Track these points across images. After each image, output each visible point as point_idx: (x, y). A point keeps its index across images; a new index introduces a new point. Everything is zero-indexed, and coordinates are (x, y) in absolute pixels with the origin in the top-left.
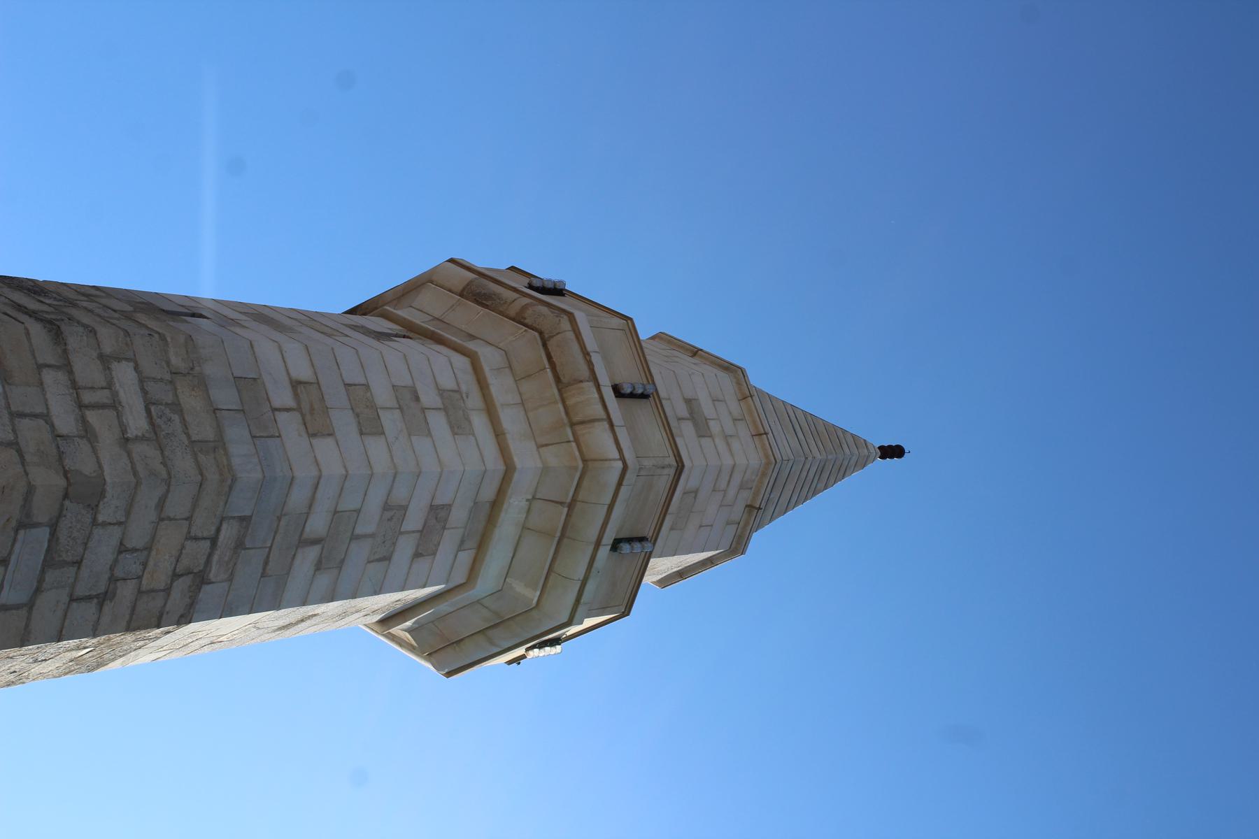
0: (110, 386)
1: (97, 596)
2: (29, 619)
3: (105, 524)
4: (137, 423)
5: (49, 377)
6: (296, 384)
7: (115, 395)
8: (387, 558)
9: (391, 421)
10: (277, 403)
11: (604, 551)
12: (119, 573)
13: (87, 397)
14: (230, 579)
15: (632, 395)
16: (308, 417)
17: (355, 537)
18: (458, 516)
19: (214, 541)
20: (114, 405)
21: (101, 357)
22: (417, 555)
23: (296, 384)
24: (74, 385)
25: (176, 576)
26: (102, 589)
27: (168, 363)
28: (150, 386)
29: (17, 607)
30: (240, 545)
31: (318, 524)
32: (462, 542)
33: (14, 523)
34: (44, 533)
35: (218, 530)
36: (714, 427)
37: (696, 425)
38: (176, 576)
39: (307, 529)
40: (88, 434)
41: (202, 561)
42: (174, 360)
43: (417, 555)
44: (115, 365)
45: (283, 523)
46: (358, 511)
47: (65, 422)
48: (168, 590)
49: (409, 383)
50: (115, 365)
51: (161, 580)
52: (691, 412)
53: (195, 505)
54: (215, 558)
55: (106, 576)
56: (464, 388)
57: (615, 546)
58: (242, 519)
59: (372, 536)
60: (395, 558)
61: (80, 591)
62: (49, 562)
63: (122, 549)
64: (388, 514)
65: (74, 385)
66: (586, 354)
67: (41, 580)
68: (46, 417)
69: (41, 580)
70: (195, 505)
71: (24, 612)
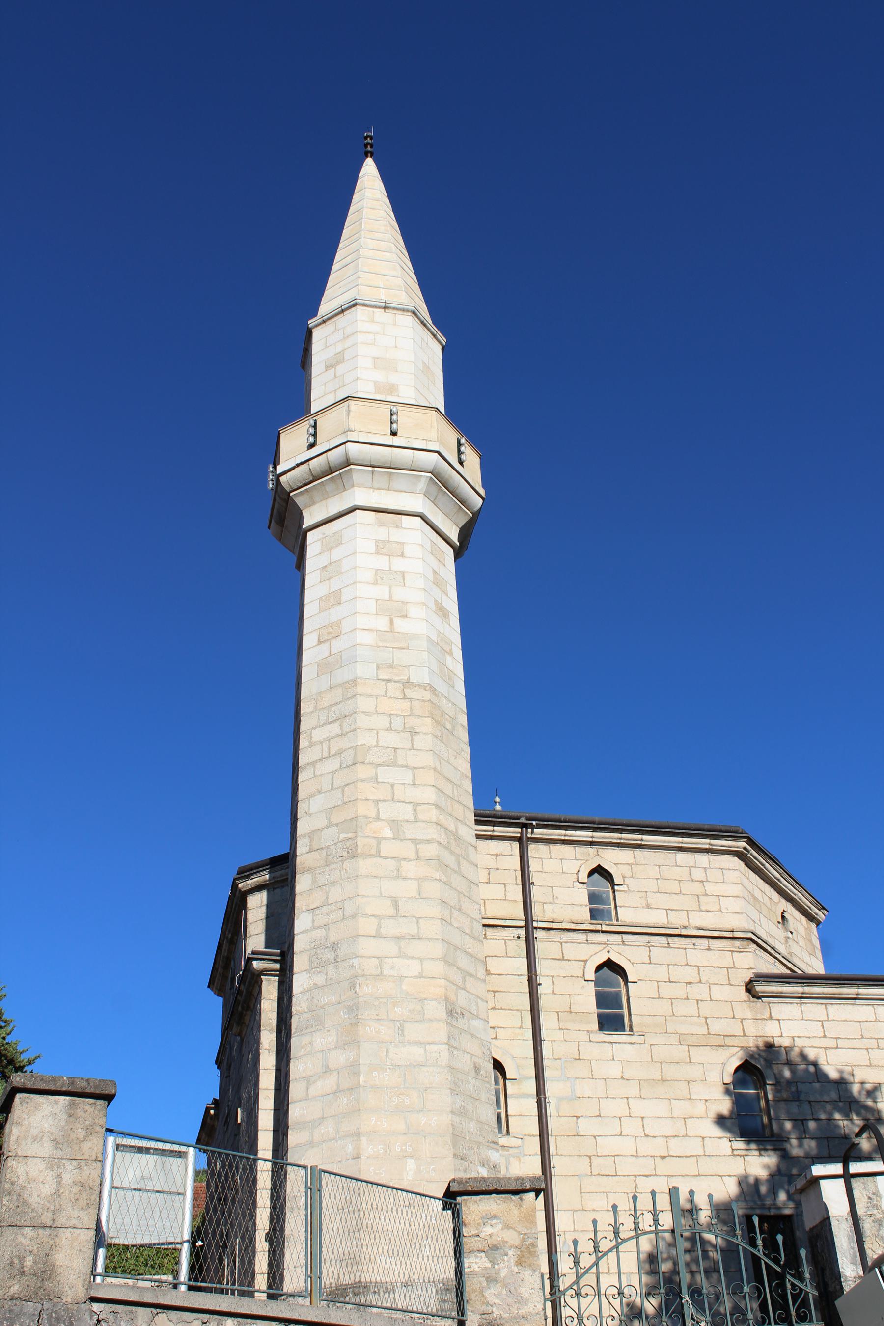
0: (321, 742)
1: (411, 736)
2: (420, 768)
3: (377, 741)
4: (335, 729)
5: (318, 773)
6: (320, 642)
7: (325, 740)
8: (403, 573)
9: (335, 584)
10: (327, 653)
11: (396, 441)
12: (401, 728)
13: (326, 754)
14: (407, 667)
15: (315, 435)
16: (334, 635)
17: (391, 599)
18: (382, 533)
19: (388, 681)
20: (328, 739)
21: (310, 746)
22: (402, 555)
23: (320, 642)
24: (321, 760)
25: (404, 697)
26: (409, 734)
27: (312, 712)
28: (321, 723)
29: (414, 775)
30: (391, 666)
31: (382, 623)
32: (397, 527)
33: (375, 785)
34: (380, 769)
35: (383, 680)
36: (339, 348)
37: (338, 363)
38: (404, 697)
39: (385, 629)
40: (340, 753)
41: (398, 685)
42: (311, 709)
43: (402, 555)
44: (314, 740)
45: (380, 644)
46: (377, 600)
47: (333, 764)
48: (411, 700)
49: (318, 571)
50: (314, 740)
51: (406, 704)
52: (332, 366)
53: (371, 696)
54: (397, 678)
55: (402, 734)
56: (321, 536)
57: (394, 434)
58: (378, 668)
59: (390, 588)
60: (402, 569)
61: (409, 746)
62: (394, 764)
63: (390, 729)
64: (380, 581)
65: (321, 760)
66: (298, 465)
67: (402, 766)
68: (334, 772)
69: (402, 766)
70: (371, 696)
71: (416, 771)
